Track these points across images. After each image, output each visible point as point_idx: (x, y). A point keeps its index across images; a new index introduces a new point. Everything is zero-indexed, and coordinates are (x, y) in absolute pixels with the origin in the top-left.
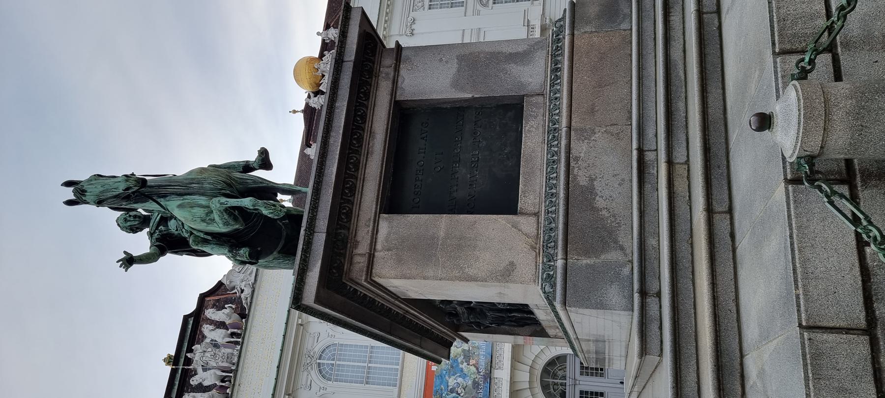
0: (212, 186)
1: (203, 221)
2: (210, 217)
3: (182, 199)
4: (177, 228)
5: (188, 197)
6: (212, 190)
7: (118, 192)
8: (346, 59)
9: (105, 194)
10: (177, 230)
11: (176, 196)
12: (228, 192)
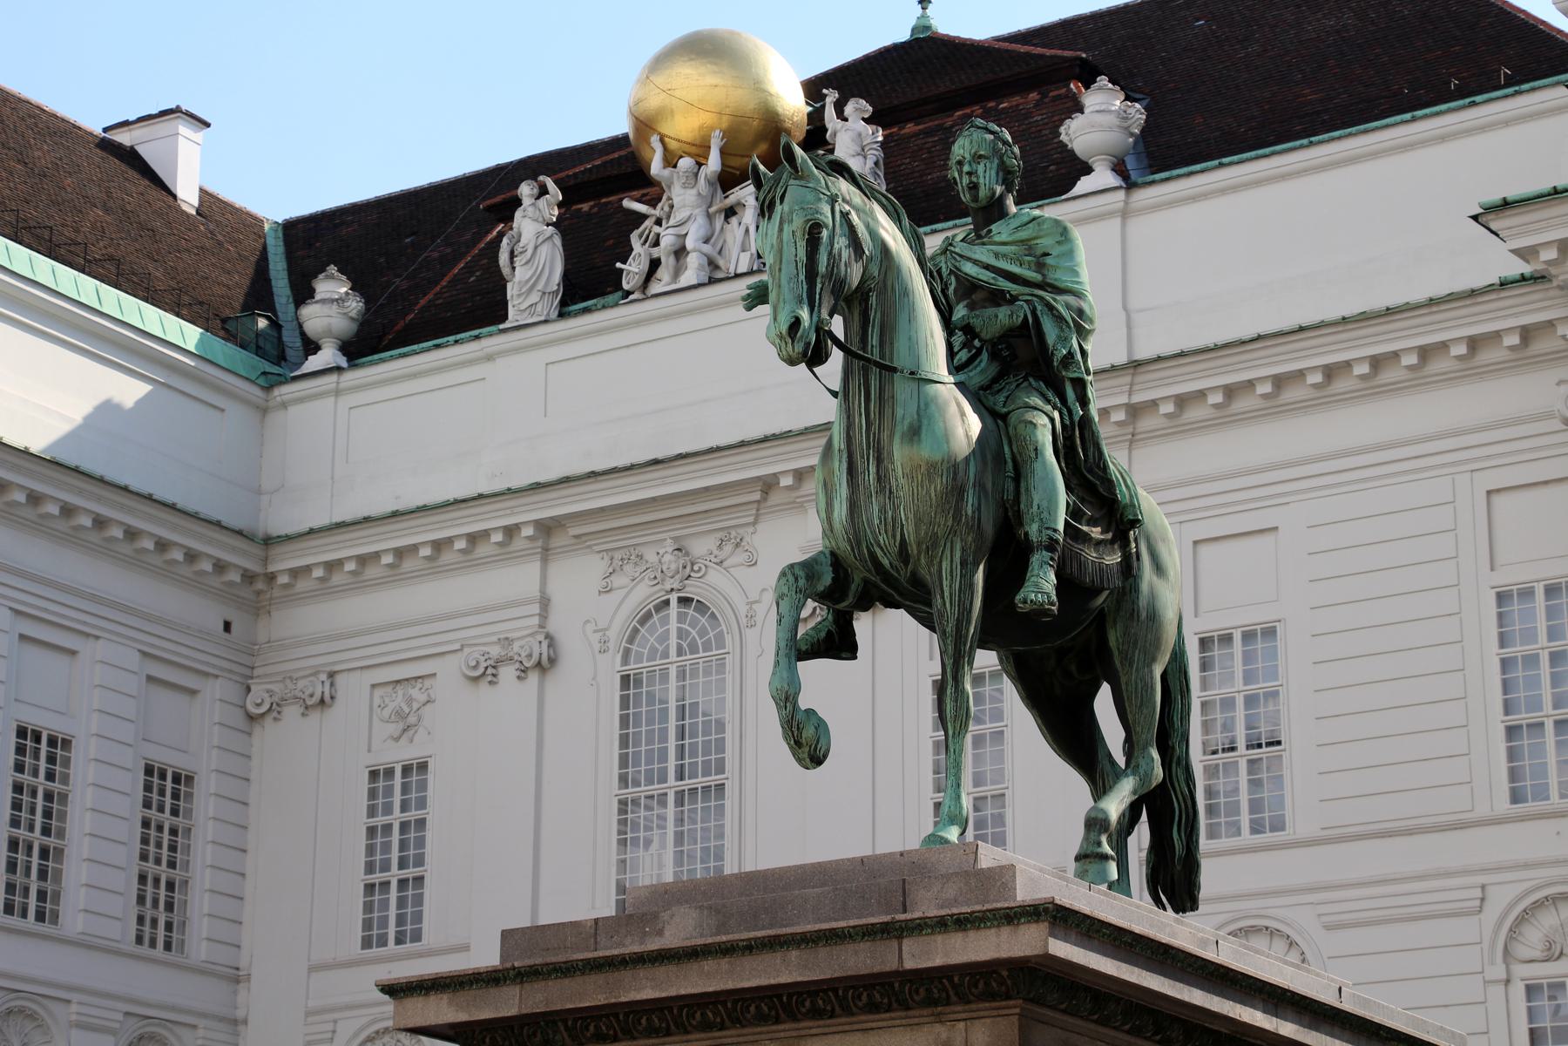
0: (876, 522)
3: (842, 447)
5: (845, 466)
6: (868, 524)
8: (907, 944)
12: (886, 562)
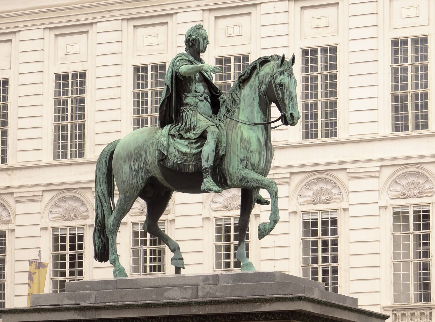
1: (247, 159)
2: (249, 165)
3: (264, 144)
4: (198, 92)
6: (266, 171)
7: (287, 105)
9: (288, 94)
10: (196, 91)
11: (265, 139)
